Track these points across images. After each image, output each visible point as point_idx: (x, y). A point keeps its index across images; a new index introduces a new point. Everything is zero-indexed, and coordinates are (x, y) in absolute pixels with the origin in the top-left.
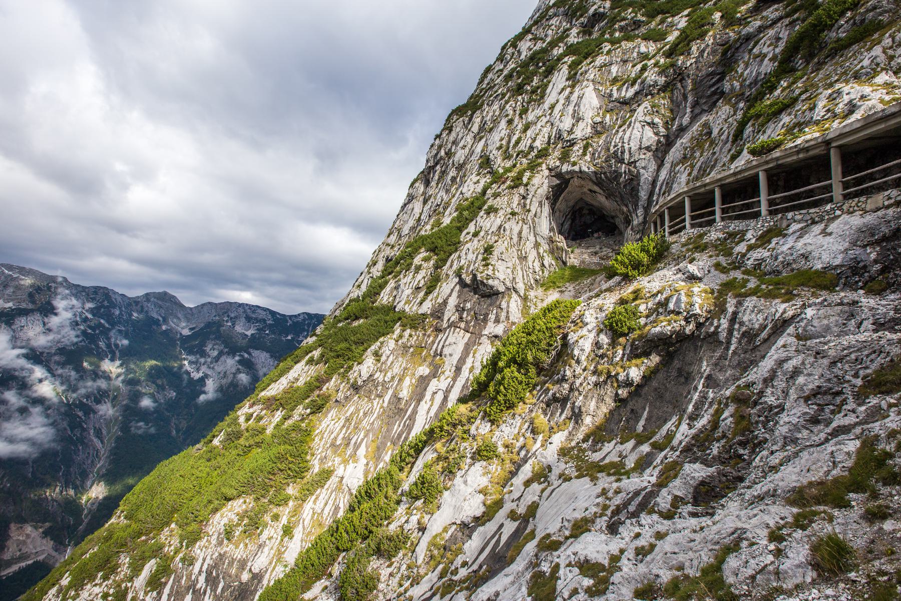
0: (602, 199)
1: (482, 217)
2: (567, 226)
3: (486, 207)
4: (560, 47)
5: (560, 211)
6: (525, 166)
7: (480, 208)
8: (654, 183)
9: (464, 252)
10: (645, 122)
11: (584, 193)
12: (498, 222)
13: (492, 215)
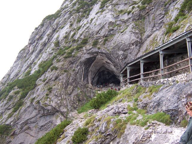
0: (113, 67)
1: (49, 72)
2: (96, 79)
5: (92, 72)
6: (75, 47)
7: (49, 67)
10: (132, 32)
13: (54, 71)
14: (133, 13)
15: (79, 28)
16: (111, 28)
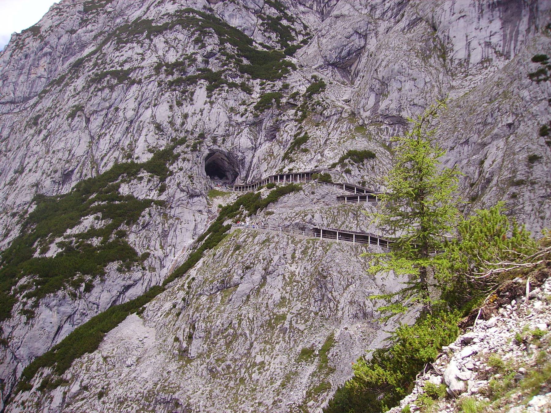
3: (181, 157)
8: (251, 162)
9: (176, 176)
11: (219, 159)
12: (190, 165)
14: (247, 117)
15: (186, 116)
16: (227, 128)
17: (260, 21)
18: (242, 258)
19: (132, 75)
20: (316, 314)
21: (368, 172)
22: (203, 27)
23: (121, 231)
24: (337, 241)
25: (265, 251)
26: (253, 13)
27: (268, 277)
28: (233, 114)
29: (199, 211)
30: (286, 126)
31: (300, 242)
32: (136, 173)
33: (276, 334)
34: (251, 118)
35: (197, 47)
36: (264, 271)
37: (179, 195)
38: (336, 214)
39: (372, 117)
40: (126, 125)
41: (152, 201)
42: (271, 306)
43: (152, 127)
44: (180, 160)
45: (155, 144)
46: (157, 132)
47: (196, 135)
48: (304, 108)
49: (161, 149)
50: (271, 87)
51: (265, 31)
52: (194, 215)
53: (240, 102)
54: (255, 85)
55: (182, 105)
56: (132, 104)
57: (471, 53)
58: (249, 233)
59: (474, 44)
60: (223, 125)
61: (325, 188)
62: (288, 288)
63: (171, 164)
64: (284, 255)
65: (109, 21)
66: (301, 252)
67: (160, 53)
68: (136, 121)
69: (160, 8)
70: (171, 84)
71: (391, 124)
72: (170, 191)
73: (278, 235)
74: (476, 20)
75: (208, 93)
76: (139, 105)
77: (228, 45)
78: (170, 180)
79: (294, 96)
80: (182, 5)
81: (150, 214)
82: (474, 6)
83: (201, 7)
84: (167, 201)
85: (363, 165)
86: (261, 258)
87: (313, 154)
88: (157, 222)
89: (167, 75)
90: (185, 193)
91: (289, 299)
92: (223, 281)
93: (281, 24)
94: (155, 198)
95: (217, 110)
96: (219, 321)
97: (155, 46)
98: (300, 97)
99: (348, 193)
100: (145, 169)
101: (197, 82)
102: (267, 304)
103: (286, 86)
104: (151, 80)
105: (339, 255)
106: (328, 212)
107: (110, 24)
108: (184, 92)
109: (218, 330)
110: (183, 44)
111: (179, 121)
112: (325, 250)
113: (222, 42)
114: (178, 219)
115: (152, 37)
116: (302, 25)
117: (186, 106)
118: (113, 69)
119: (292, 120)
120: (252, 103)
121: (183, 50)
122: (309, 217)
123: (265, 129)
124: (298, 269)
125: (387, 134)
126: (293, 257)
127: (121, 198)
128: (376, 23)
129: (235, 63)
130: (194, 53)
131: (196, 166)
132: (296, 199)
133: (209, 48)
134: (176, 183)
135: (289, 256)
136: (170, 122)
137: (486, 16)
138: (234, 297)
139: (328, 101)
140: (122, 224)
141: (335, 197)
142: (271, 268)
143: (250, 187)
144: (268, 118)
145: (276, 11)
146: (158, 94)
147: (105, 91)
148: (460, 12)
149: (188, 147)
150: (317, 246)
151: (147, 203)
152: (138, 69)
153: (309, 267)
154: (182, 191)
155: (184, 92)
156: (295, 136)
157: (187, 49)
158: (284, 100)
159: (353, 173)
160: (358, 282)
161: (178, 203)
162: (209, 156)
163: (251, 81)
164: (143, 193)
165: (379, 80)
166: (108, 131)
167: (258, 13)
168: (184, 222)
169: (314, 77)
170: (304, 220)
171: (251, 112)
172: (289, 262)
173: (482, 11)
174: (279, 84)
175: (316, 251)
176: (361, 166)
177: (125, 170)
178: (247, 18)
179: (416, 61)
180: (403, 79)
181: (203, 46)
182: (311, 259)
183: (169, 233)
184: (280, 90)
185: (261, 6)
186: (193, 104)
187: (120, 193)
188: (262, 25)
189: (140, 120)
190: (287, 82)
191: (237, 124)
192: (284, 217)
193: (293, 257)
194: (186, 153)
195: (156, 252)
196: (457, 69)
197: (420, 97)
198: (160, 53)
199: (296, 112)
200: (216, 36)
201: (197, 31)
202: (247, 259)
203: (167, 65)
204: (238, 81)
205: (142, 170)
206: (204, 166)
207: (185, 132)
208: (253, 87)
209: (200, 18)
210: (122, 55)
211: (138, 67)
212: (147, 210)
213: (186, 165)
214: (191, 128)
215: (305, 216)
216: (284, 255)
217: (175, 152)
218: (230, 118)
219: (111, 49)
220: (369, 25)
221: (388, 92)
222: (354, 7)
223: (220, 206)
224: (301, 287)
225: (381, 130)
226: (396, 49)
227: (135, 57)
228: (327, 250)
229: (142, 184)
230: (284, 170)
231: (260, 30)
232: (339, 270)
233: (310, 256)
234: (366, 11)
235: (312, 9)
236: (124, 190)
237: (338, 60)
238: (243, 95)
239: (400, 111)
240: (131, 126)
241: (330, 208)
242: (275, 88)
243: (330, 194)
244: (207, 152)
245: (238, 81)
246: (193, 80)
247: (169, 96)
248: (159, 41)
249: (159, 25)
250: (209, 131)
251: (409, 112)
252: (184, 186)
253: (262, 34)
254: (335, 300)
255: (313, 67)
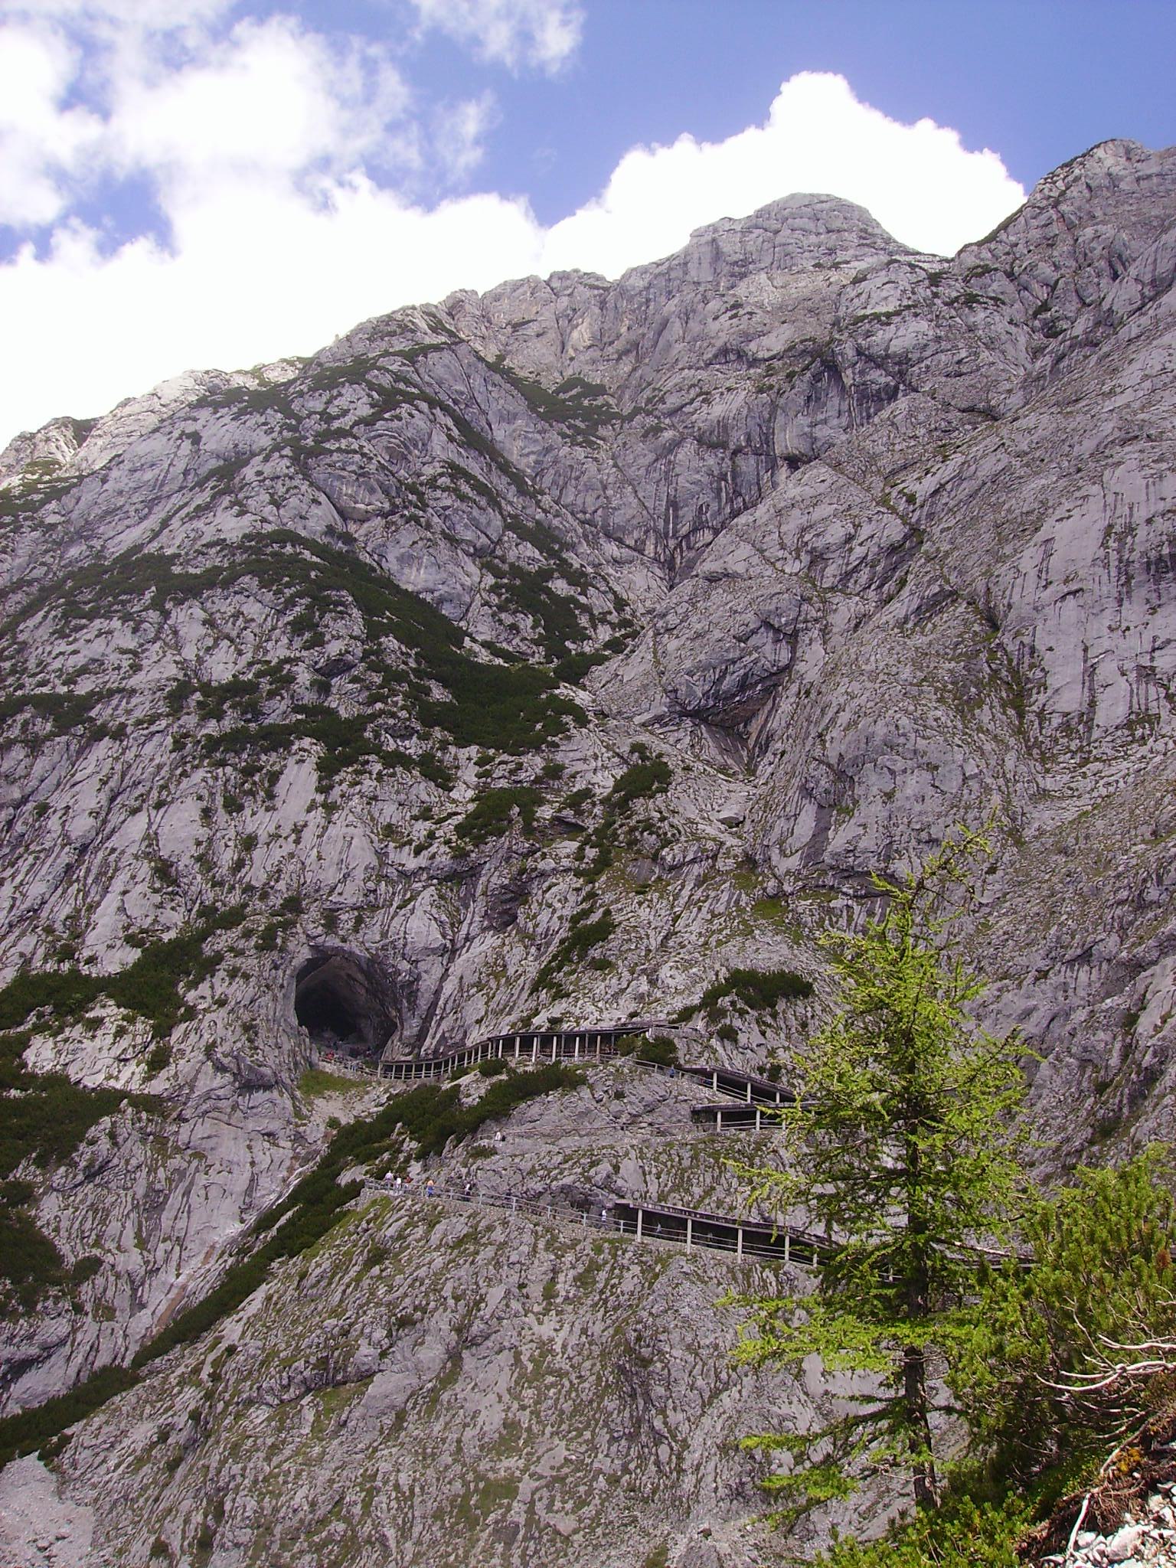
3: (223, 965)
4: (283, 698)
8: (437, 993)
9: (205, 1023)
14: (433, 857)
15: (249, 843)
16: (371, 885)
17: (490, 580)
18: (390, 1289)
19: (100, 713)
20: (613, 1481)
21: (788, 1037)
22: (321, 585)
23: (17, 1184)
24: (689, 1247)
25: (462, 1272)
26: (468, 554)
27: (465, 1354)
28: (392, 845)
29: (269, 1134)
30: (549, 888)
31: (573, 1247)
32: (84, 1005)
33: (481, 1543)
34: (444, 859)
35: (298, 643)
36: (454, 1336)
37: (210, 1081)
38: (686, 1163)
39: (805, 872)
40: (66, 857)
41: (123, 1094)
42: (471, 1450)
43: (145, 869)
44: (222, 974)
45: (149, 920)
46: (157, 885)
47: (276, 901)
48: (603, 837)
49: (166, 937)
50: (512, 772)
51: (502, 608)
52: (249, 1147)
53: (415, 811)
54: (462, 761)
55: (240, 808)
56: (90, 797)
57: (1099, 697)
58: (416, 1213)
59: (1107, 670)
60: (359, 874)
61: (658, 1082)
62: (529, 1393)
63: (193, 985)
64: (522, 1286)
65: (47, 551)
66: (575, 1279)
67: (190, 653)
68: (97, 849)
69: (199, 524)
70: (212, 744)
71: (862, 897)
72: (183, 1067)
73: (505, 1223)
74: (1112, 604)
75: (320, 779)
76: (112, 799)
77: (391, 642)
78: (186, 1034)
79: (577, 801)
80: (264, 520)
81: (112, 1136)
82: (1107, 566)
83: (321, 528)
84: (170, 1099)
85: (774, 1016)
86: (447, 1292)
87: (626, 975)
88: (134, 1162)
89: (204, 718)
90: (228, 1077)
91: (529, 1429)
92: (323, 1362)
93: (549, 592)
94: (135, 1087)
95: (344, 830)
96: (301, 1493)
97: (176, 633)
98: (594, 804)
99: (725, 1100)
100: (109, 996)
101: (293, 743)
102: (459, 1441)
103: (554, 772)
104: (153, 728)
105: (691, 1293)
106: (664, 1158)
107: (48, 559)
108: (248, 772)
109: (295, 1523)
110: (257, 631)
111: (227, 857)
112: (650, 1276)
113: (374, 632)
114: (199, 1155)
115: (169, 605)
116: (611, 596)
117: (254, 814)
118: (45, 690)
119: (567, 870)
120: (451, 815)
121: (258, 647)
122: (605, 1168)
123: (484, 894)
124: (563, 1334)
125: (849, 924)
126: (549, 1294)
127: (28, 1080)
128: (824, 602)
129: (406, 696)
130: (288, 660)
131: (269, 996)
132: (567, 1113)
133: (334, 648)
134: (202, 1044)
135: (536, 1290)
136: (199, 859)
137: (1141, 593)
138: (357, 1414)
139: (676, 821)
140: (24, 1162)
141: (685, 1110)
142: (474, 1330)
143: (428, 1068)
144: (495, 862)
145: (537, 553)
146: (172, 771)
147: (13, 754)
148: (1066, 581)
149: (247, 934)
150: (625, 1262)
151: (108, 1101)
152: (118, 696)
153: (597, 1329)
154: (220, 1068)
155: (248, 772)
156: (575, 920)
157: (270, 645)
158: (546, 812)
159: (742, 1039)
160: (749, 1381)
161: (205, 1107)
162: (311, 965)
163: (452, 749)
164: (97, 1067)
165: (829, 765)
166: (9, 871)
167: (484, 557)
168: (217, 1167)
169: (639, 748)
170: (589, 1179)
171: (448, 842)
172: (536, 1308)
173: (1129, 578)
174: (534, 764)
175: (621, 1277)
176: (769, 1020)
177: (49, 995)
178: (451, 567)
179: (939, 713)
180: (899, 764)
181: (318, 641)
182: (606, 1301)
183: (167, 1197)
184: (538, 780)
185: (494, 537)
186: (274, 809)
187: (25, 1065)
188: (494, 589)
189: (109, 844)
190: (559, 757)
191: (403, 874)
192: (526, 1166)
193: (549, 1294)
194: (239, 953)
195: (121, 1258)
196: (1056, 741)
197: (949, 821)
198: (190, 653)
199: (581, 849)
200: (356, 613)
201: (300, 595)
202: (406, 1295)
203: (206, 688)
204: (413, 747)
205: (102, 997)
206: (293, 995)
207: (244, 892)
208: (457, 768)
209: (315, 559)
210: (75, 652)
211: (119, 691)
212: (106, 1121)
213: (238, 991)
214: (263, 877)
215: (593, 1164)
216: (522, 1286)
217: (207, 949)
218: (381, 855)
219: (44, 633)
220: (805, 607)
221: (856, 802)
222: (761, 551)
223: (333, 1123)
224: (569, 1392)
225: (830, 911)
226: (882, 677)
227: (114, 658)
228: (656, 1276)
229: (97, 1042)
230: (536, 1021)
231: (486, 603)
232: (689, 1339)
233: (602, 1292)
234: (797, 566)
235: (641, 552)
236: (41, 1055)
237: (711, 703)
238: (424, 791)
239: (888, 858)
240: (80, 861)
241: (670, 1144)
242: (523, 775)
243: (671, 1101)
244: (305, 954)
245: (413, 747)
246: (278, 739)
247: (204, 780)
248: (188, 619)
249: (192, 571)
250: (317, 891)
251: (916, 861)
252: (226, 1056)
253: (493, 615)
254: (674, 1437)
255: (638, 720)
